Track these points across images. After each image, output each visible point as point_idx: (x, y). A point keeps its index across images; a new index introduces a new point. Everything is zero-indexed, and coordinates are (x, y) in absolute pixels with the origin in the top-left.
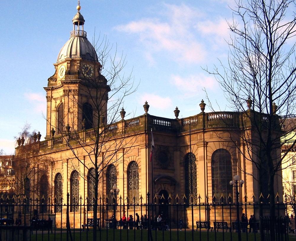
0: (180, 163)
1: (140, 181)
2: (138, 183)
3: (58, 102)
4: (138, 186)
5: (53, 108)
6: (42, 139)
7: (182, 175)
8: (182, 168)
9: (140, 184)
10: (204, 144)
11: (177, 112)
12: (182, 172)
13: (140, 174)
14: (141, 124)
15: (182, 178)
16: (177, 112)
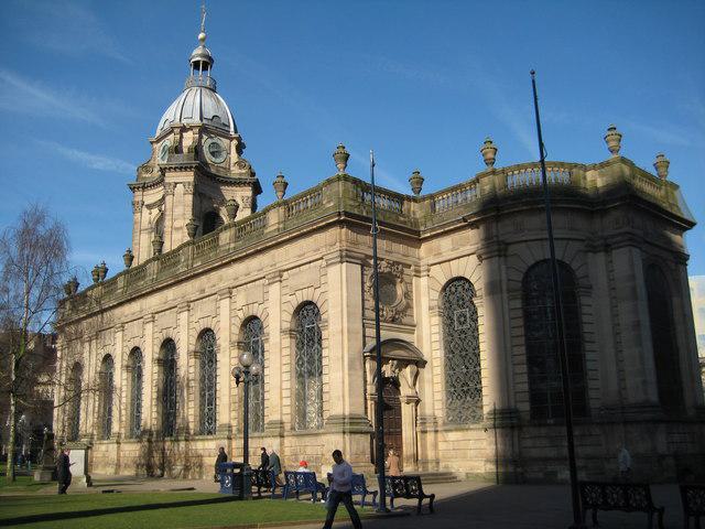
0: (430, 308)
1: (325, 353)
2: (321, 357)
3: (155, 211)
4: (321, 366)
5: (145, 224)
6: (109, 276)
7: (436, 337)
8: (436, 320)
9: (325, 362)
10: (499, 250)
11: (418, 182)
12: (436, 329)
13: (325, 334)
14: (329, 202)
15: (436, 346)
16: (418, 182)
